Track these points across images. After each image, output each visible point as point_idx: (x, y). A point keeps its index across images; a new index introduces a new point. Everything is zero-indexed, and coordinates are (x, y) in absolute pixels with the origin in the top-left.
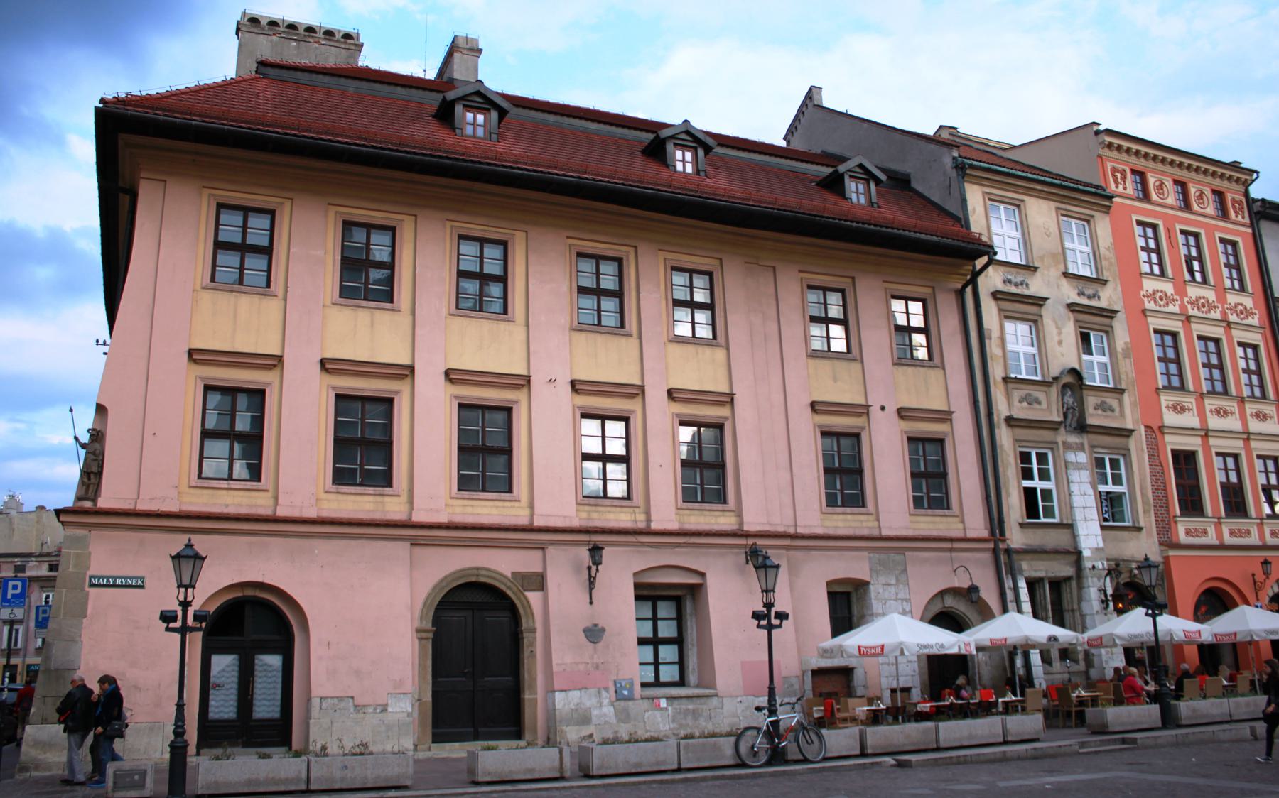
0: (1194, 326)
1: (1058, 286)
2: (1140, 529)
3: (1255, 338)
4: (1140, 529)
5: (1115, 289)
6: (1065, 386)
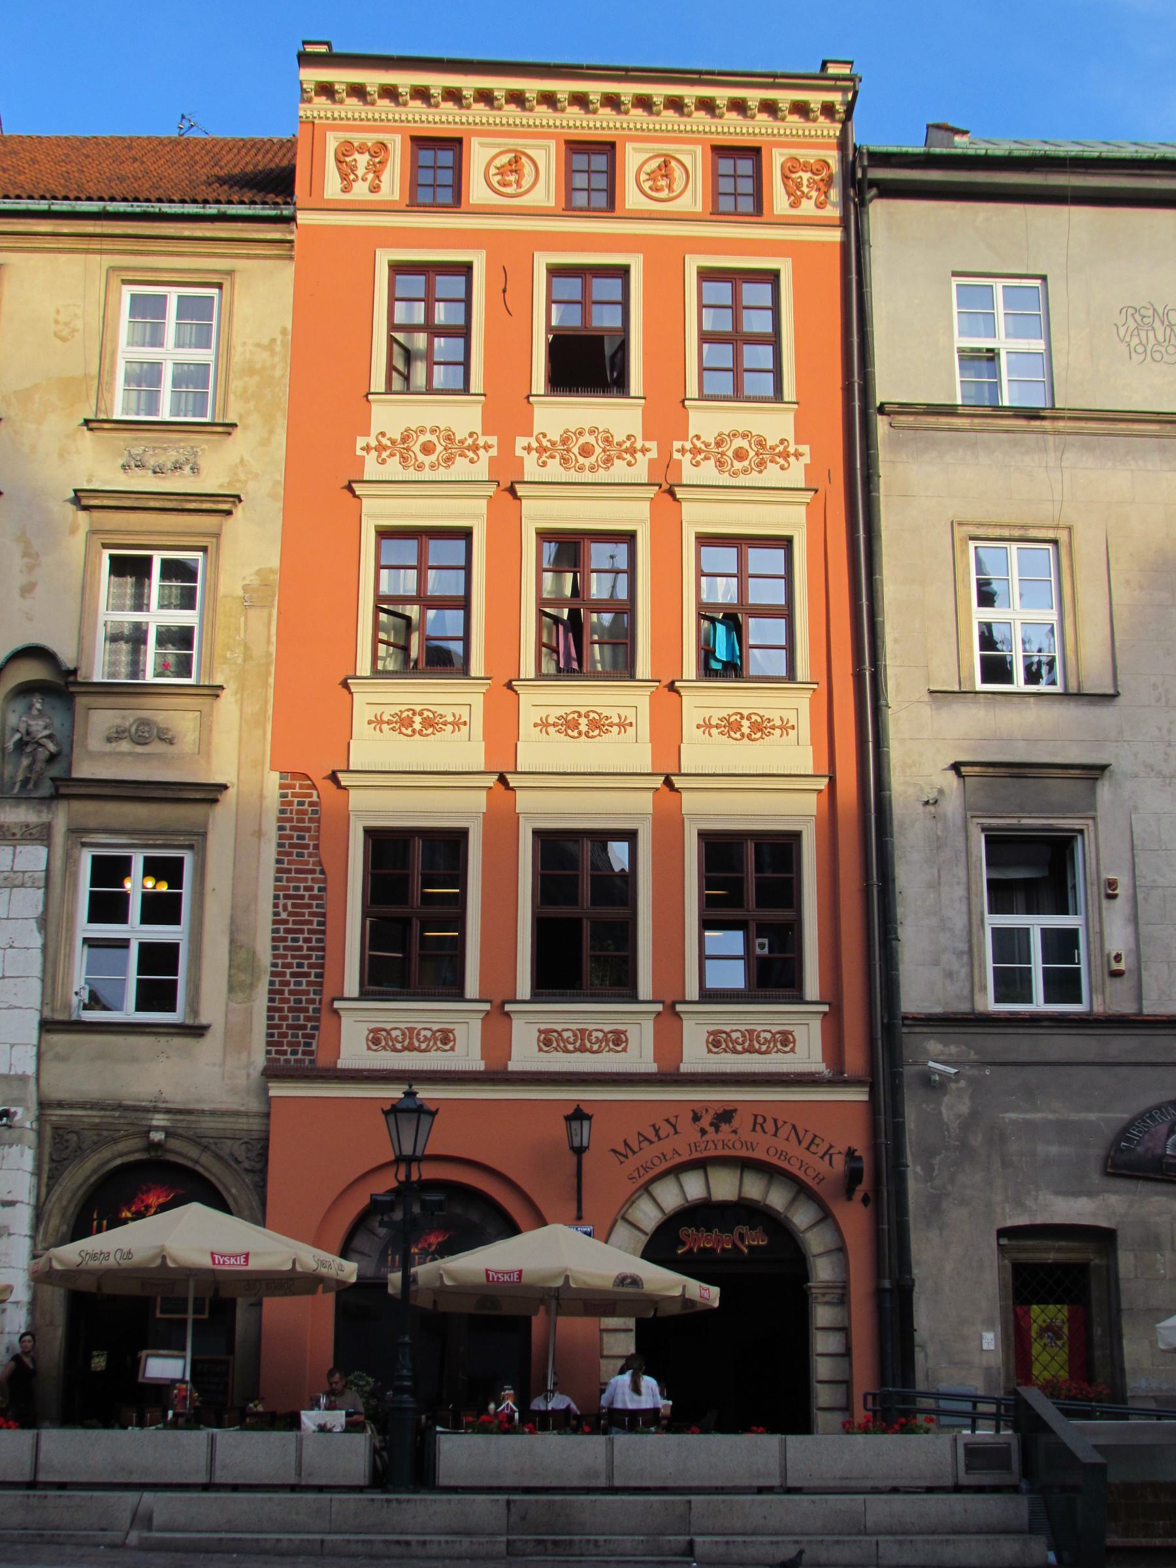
0: (688, 510)
1: (62, 455)
2: (197, 1031)
3: (790, 518)
4: (197, 1031)
5: (265, 442)
6: (26, 690)
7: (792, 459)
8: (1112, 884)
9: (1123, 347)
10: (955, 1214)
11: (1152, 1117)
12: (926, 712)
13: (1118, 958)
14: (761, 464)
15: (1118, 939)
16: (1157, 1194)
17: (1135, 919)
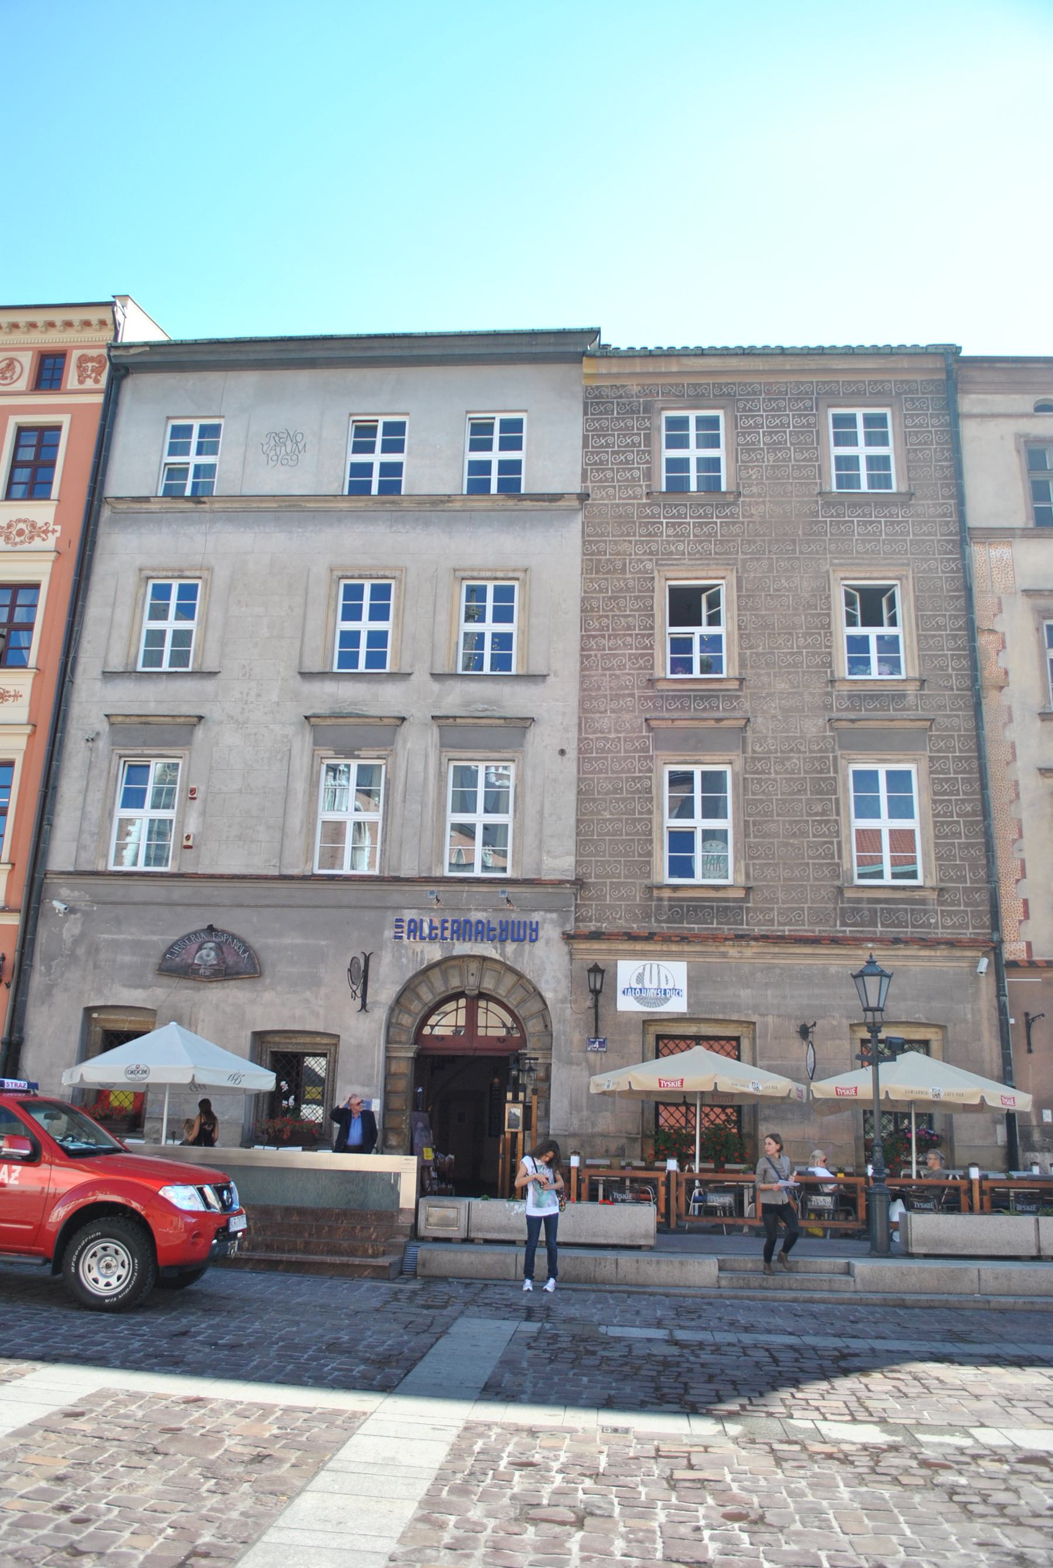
7: (50, 534)
8: (193, 791)
9: (265, 457)
10: (60, 997)
11: (189, 939)
12: (98, 685)
13: (188, 838)
14: (32, 538)
15: (192, 826)
16: (187, 988)
17: (203, 813)
